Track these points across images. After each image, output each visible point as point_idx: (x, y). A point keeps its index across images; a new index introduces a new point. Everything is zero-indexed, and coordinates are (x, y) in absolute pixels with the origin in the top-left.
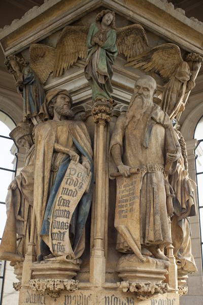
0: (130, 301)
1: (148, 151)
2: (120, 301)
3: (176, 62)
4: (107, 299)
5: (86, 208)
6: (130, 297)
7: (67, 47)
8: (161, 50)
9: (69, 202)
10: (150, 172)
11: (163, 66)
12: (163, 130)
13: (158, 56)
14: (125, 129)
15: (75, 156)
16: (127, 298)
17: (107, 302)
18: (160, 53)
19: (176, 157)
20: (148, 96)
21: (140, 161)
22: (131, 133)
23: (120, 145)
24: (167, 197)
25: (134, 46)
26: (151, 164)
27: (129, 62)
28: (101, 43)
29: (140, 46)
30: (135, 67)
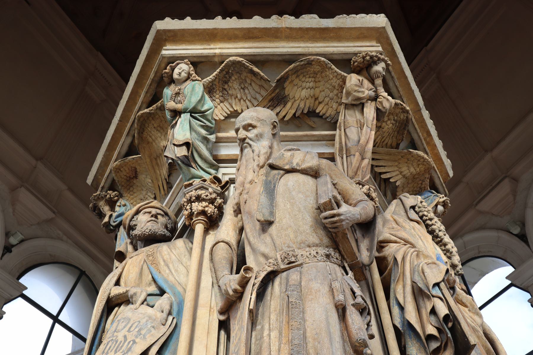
1: (273, 229)
3: (336, 82)
7: (154, 144)
8: (294, 77)
10: (283, 266)
11: (316, 99)
13: (296, 87)
14: (238, 211)
15: (135, 294)
18: (296, 81)
19: (339, 215)
20: (259, 137)
22: (244, 211)
23: (227, 243)
24: (342, 311)
25: (246, 91)
26: (286, 249)
29: (257, 88)
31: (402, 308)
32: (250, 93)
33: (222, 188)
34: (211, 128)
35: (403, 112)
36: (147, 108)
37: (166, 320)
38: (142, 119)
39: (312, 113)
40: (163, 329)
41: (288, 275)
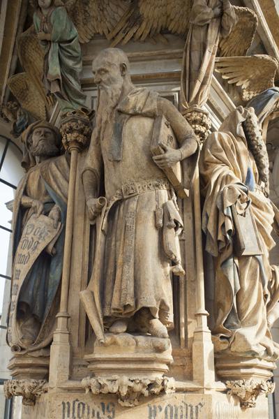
0: (108, 408)
1: (120, 167)
2: (88, 409)
4: (67, 406)
5: (54, 276)
6: (106, 402)
9: (20, 271)
10: (125, 197)
11: (168, 17)
12: (147, 123)
15: (36, 207)
16: (103, 404)
17: (66, 409)
21: (114, 185)
23: (92, 171)
25: (105, 12)
27: (113, 39)
28: (48, 37)
29: (115, 9)
30: (125, 41)
31: (208, 218)
32: (108, 14)
33: (89, 116)
34: (77, 57)
35: (251, 20)
36: (24, 30)
37: (57, 225)
38: (21, 42)
39: (164, 31)
40: (56, 232)
41: (128, 203)
